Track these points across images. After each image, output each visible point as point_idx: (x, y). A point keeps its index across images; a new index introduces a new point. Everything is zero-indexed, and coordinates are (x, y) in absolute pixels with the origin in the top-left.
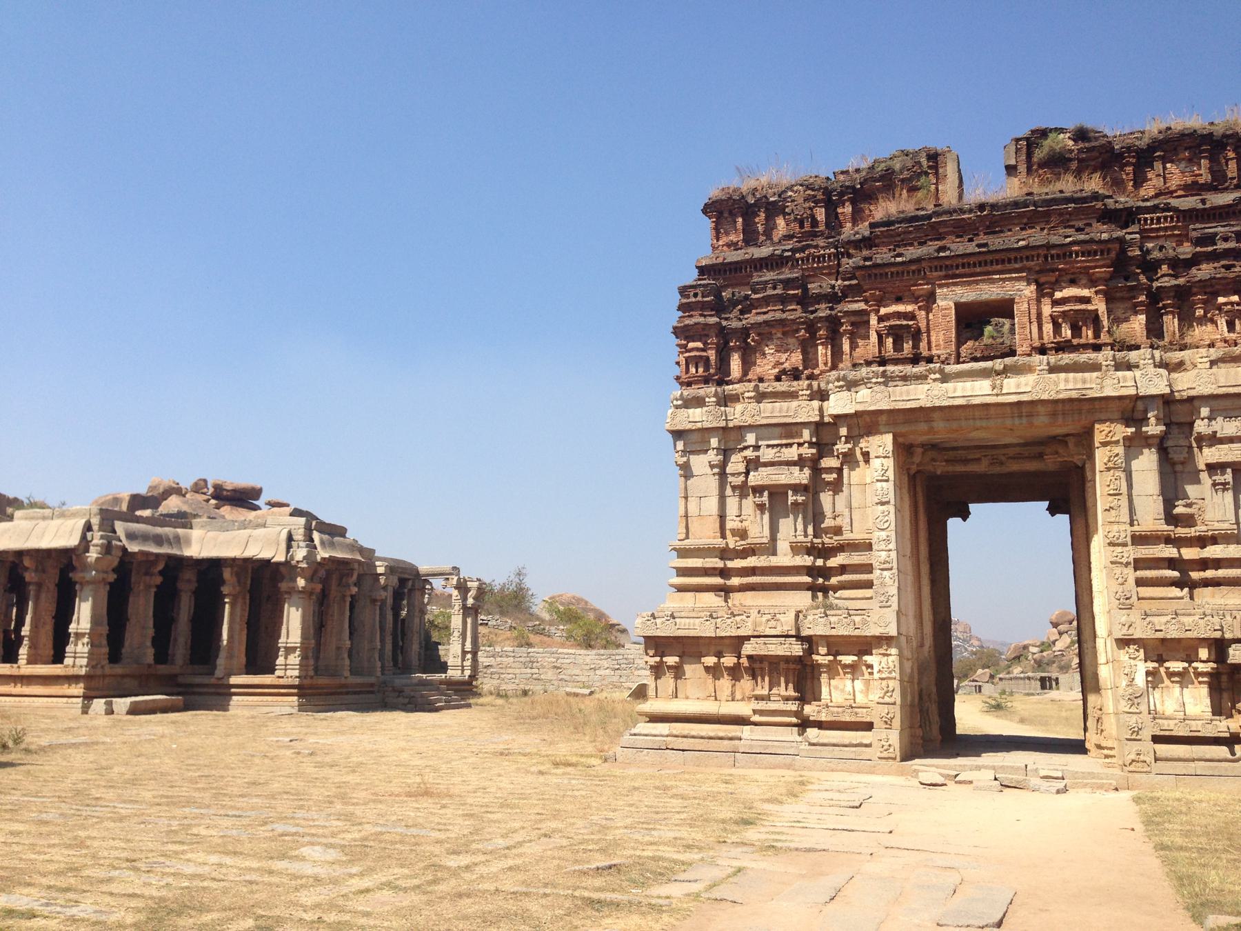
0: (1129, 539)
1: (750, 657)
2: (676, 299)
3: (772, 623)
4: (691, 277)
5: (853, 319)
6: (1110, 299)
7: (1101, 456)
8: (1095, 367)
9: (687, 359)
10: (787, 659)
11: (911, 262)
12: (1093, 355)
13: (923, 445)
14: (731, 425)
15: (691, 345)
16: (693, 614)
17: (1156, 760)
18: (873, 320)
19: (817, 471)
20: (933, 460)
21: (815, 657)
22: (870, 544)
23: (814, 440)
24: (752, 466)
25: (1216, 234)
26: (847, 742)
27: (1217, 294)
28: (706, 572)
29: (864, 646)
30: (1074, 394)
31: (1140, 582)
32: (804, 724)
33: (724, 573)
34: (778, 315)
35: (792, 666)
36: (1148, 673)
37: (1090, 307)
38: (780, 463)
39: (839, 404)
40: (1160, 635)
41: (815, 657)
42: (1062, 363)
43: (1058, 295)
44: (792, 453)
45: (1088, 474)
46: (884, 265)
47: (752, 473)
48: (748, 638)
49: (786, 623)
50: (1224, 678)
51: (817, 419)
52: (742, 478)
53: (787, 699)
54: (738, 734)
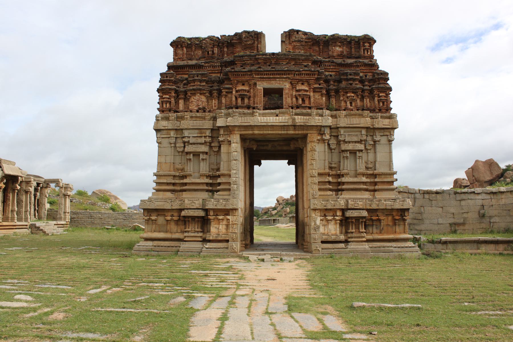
0: (316, 175)
1: (184, 217)
2: (159, 77)
3: (193, 204)
4: (165, 69)
5: (226, 91)
6: (314, 92)
7: (309, 147)
8: (309, 115)
9: (162, 102)
10: (198, 217)
11: (248, 71)
12: (309, 111)
13: (250, 139)
14: (178, 128)
15: (164, 96)
16: (165, 200)
17: (322, 249)
18: (234, 92)
19: (211, 147)
20: (253, 145)
21: (209, 217)
22: (230, 175)
23: (210, 135)
24: (186, 144)
25: (348, 73)
26: (219, 247)
27: (347, 93)
28: (168, 184)
29: (227, 212)
30: (302, 124)
31: (320, 190)
32: (205, 241)
33: (174, 184)
34: (198, 87)
35: (200, 220)
36: (321, 220)
37: (308, 94)
38: (197, 144)
39: (220, 122)
40: (325, 208)
41: (209, 217)
42: (298, 112)
43: (298, 88)
44: (202, 140)
45: (305, 152)
46: (239, 72)
47: (186, 147)
48: (184, 209)
49: (198, 204)
50: (344, 221)
51: (212, 127)
52: (182, 149)
53: (198, 232)
54: (179, 245)
